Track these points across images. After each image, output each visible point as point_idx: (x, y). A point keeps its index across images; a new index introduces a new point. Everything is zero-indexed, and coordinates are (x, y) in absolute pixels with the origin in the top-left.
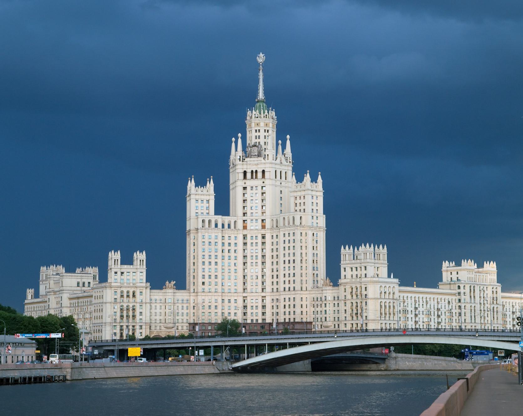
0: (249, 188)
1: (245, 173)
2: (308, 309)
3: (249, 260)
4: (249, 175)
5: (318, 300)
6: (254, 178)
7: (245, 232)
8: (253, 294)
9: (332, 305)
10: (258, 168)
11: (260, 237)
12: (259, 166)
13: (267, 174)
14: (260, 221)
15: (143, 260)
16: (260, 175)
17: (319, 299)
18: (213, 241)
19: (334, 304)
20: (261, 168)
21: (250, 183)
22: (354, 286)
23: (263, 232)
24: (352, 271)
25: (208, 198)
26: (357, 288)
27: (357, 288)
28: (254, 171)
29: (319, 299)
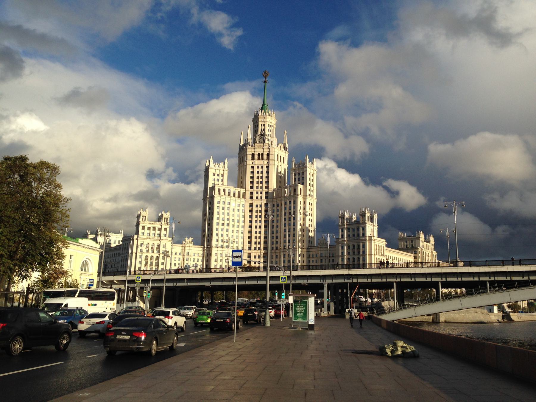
0: (256, 167)
1: (253, 155)
4: (256, 157)
6: (260, 159)
8: (255, 251)
13: (271, 156)
15: (167, 218)
16: (265, 157)
17: (315, 256)
18: (227, 206)
21: (258, 163)
25: (222, 172)
26: (354, 246)
27: (354, 246)
28: (261, 154)
29: (315, 256)
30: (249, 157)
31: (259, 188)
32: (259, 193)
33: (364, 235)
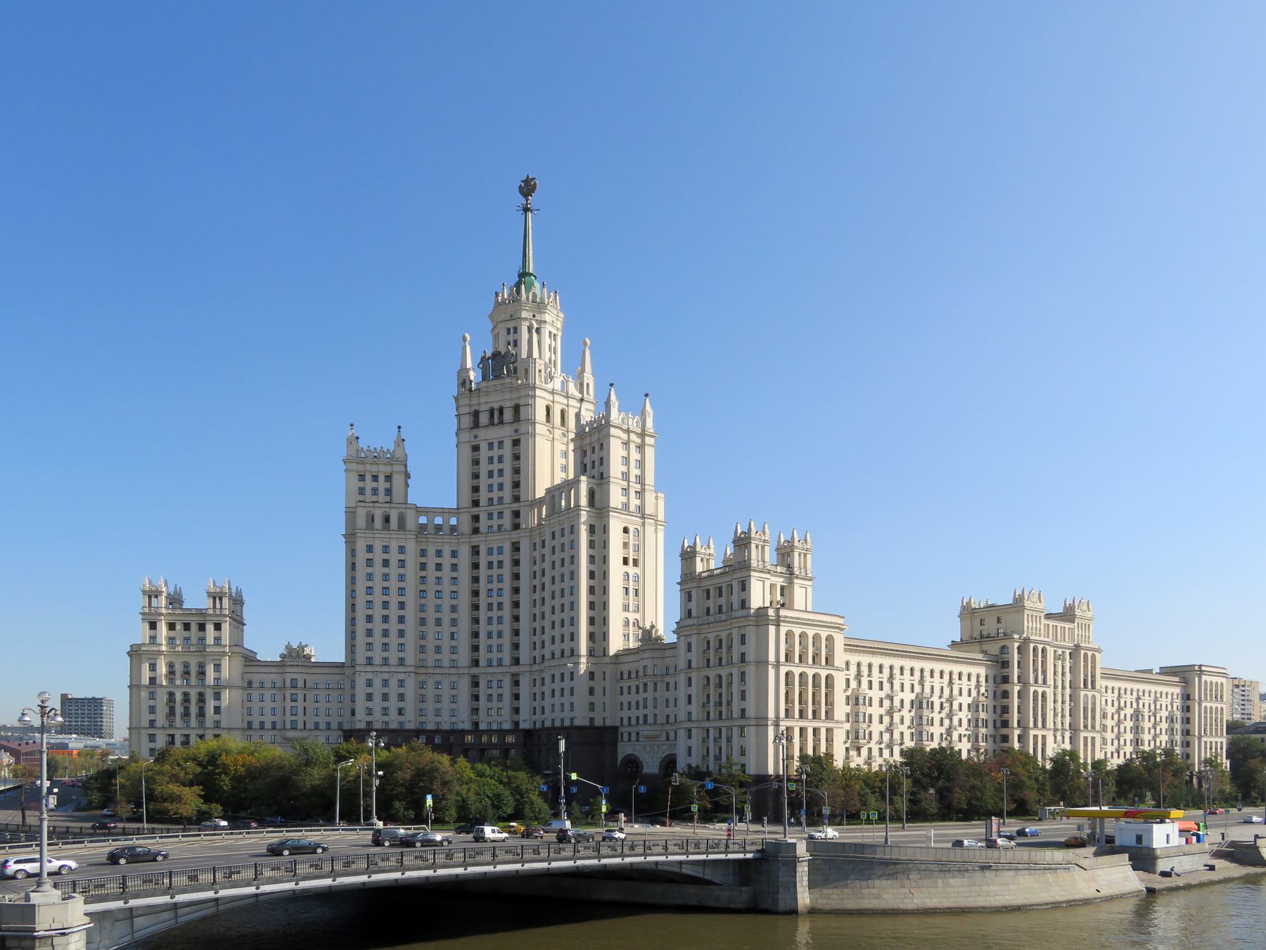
0: (484, 447)
1: (476, 414)
2: (607, 699)
3: (483, 600)
5: (632, 677)
6: (496, 423)
7: (476, 540)
9: (662, 686)
10: (504, 400)
11: (507, 547)
12: (508, 396)
14: (508, 515)
16: (508, 415)
17: (633, 675)
19: (668, 684)
20: (511, 399)
22: (711, 637)
23: (515, 536)
24: (708, 598)
30: (467, 421)
31: (495, 502)
32: (495, 515)
33: (744, 604)
